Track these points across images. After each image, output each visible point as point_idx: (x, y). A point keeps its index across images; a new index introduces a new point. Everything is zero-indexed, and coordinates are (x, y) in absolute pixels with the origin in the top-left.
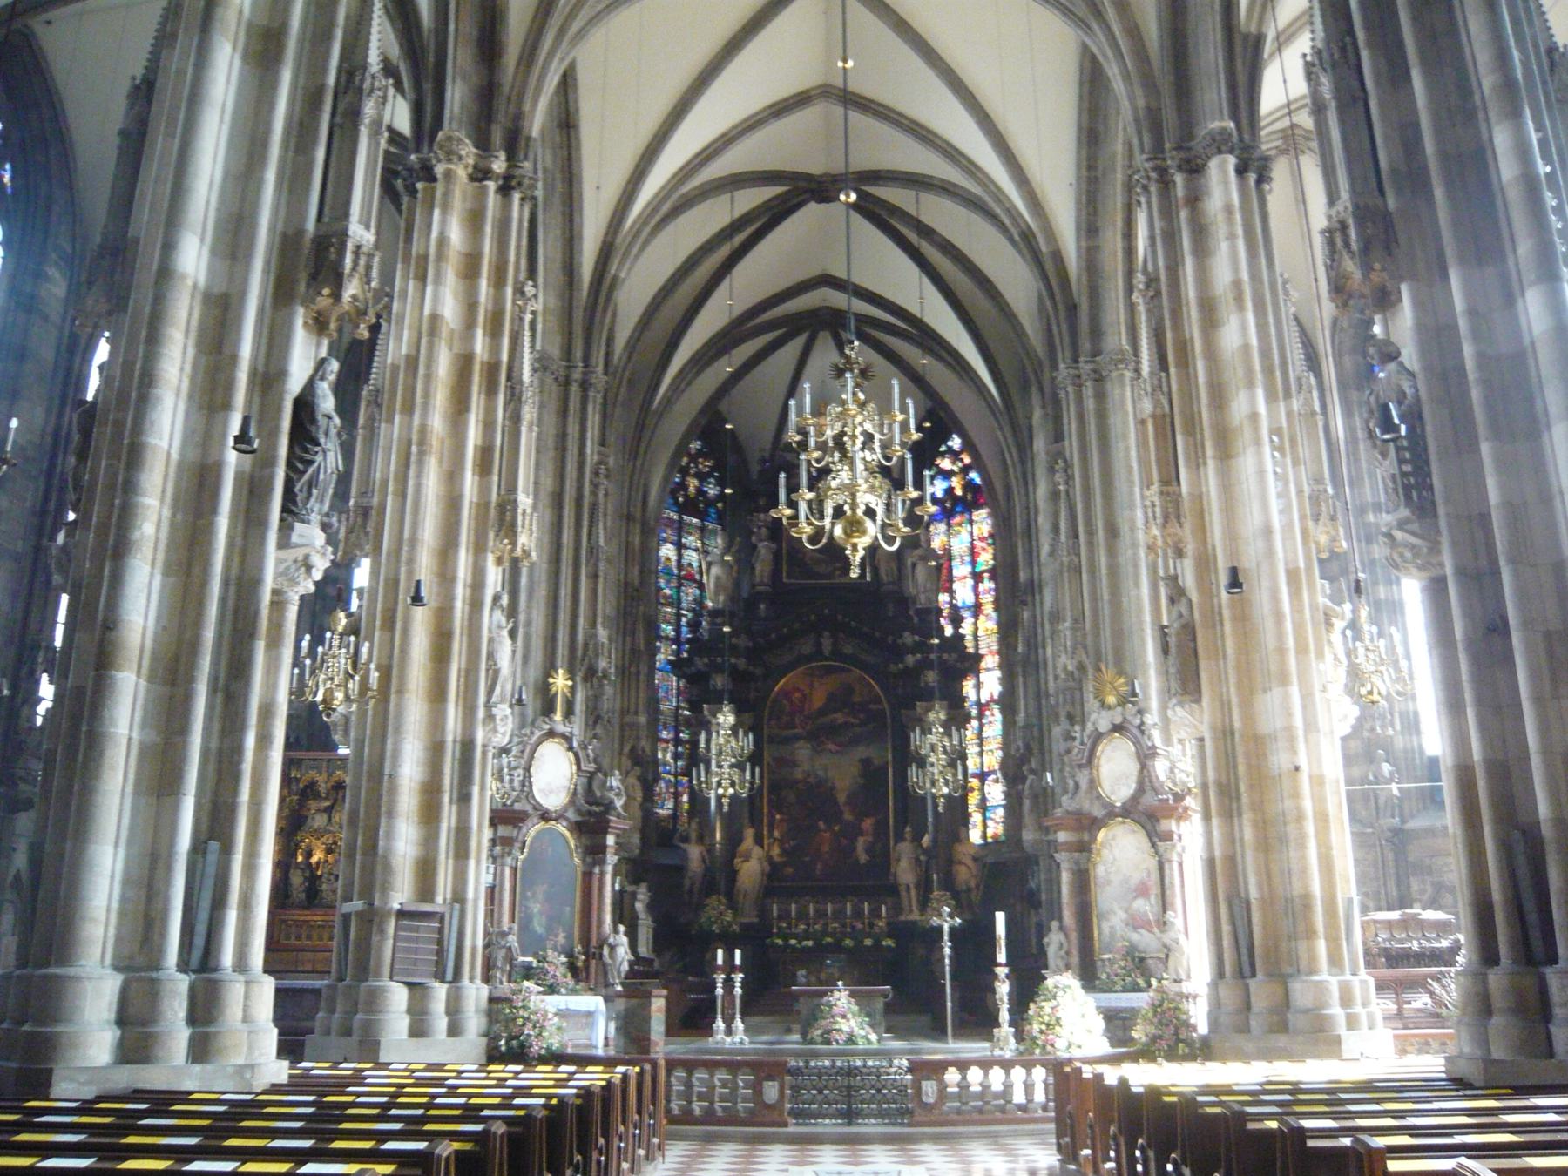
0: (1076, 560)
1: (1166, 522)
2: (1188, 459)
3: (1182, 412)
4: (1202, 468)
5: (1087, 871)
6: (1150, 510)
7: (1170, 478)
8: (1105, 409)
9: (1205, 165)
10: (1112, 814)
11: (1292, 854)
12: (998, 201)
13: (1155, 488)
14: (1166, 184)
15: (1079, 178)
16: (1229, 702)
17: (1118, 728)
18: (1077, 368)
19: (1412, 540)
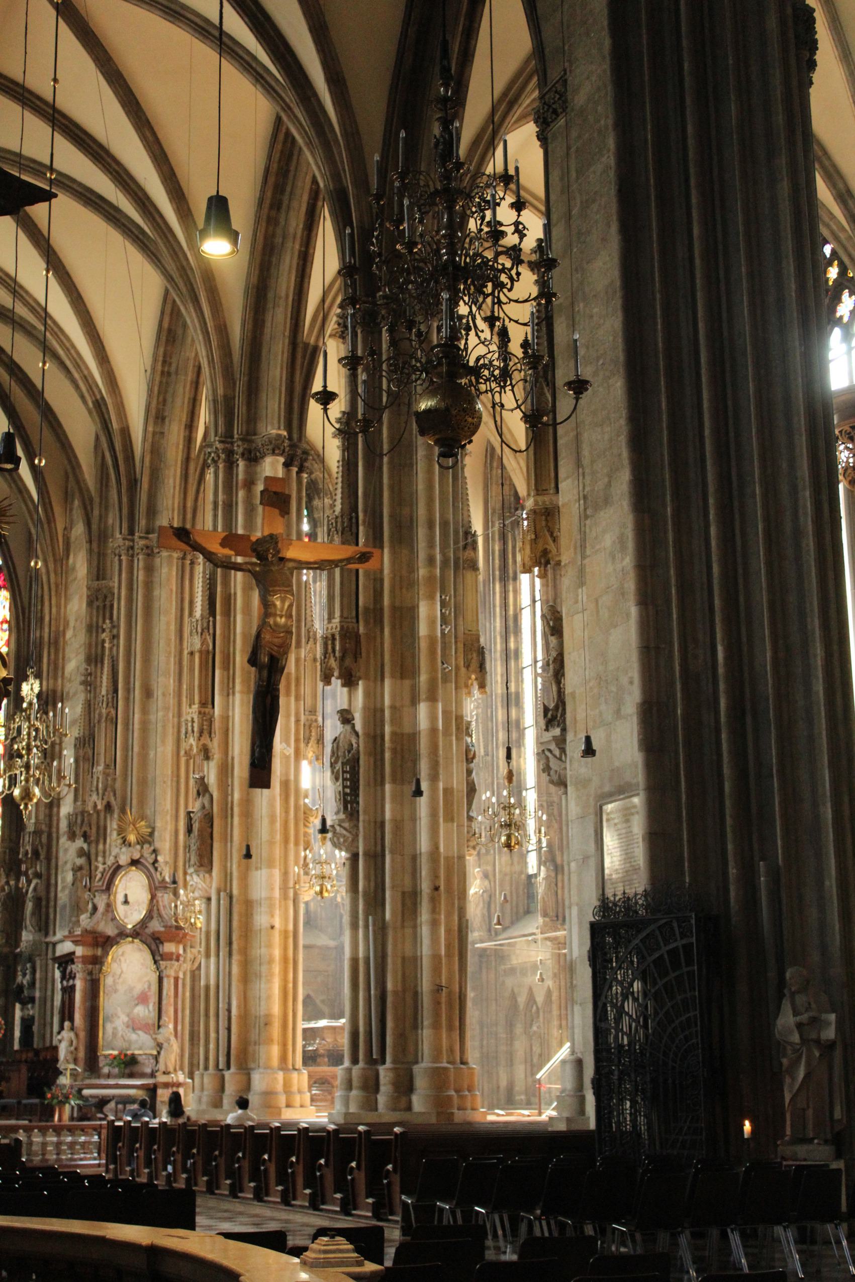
0: (113, 712)
1: (201, 736)
2: (222, 690)
3: (222, 652)
4: (231, 697)
5: (98, 980)
6: (190, 724)
7: (207, 701)
8: (152, 582)
9: (262, 457)
10: (123, 934)
11: (263, 986)
12: (77, 367)
13: (196, 707)
14: (231, 465)
15: (154, 369)
16: (231, 873)
17: (134, 863)
18: (133, 541)
19: (344, 832)
